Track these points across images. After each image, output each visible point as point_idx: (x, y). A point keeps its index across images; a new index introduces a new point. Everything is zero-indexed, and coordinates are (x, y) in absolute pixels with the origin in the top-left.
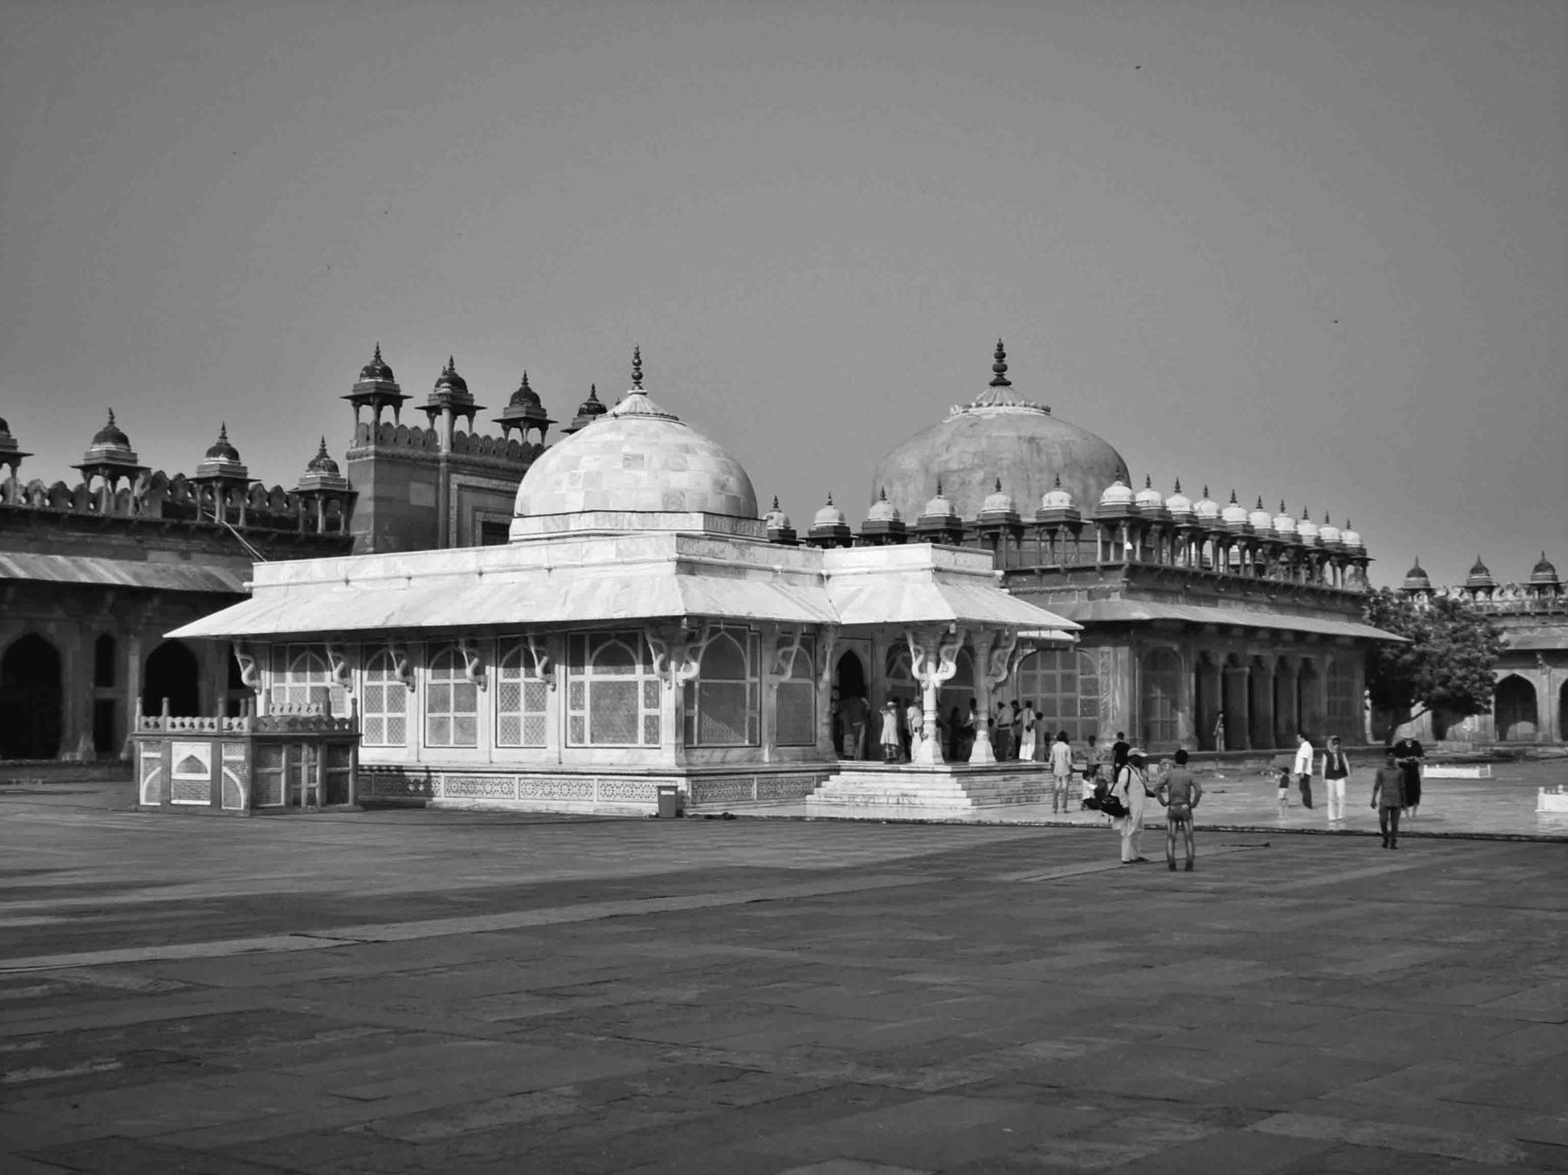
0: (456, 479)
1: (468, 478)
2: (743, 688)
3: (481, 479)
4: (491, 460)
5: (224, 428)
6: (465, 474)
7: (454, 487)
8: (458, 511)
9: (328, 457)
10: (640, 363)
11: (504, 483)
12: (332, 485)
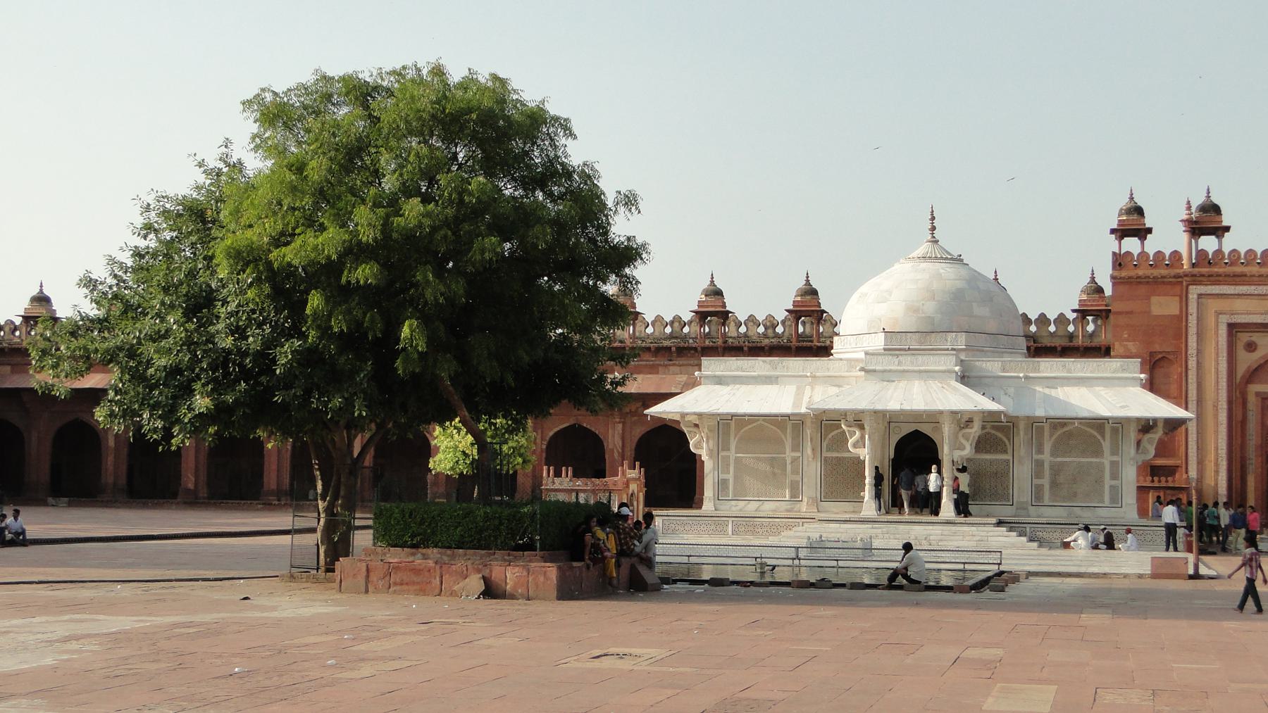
0: (1194, 291)
1: (1210, 287)
2: (784, 459)
3: (1225, 287)
4: (1238, 269)
5: (996, 272)
6: (1206, 285)
7: (1193, 297)
8: (1198, 317)
9: (1096, 283)
10: (933, 218)
11: (1253, 287)
12: (1092, 305)
